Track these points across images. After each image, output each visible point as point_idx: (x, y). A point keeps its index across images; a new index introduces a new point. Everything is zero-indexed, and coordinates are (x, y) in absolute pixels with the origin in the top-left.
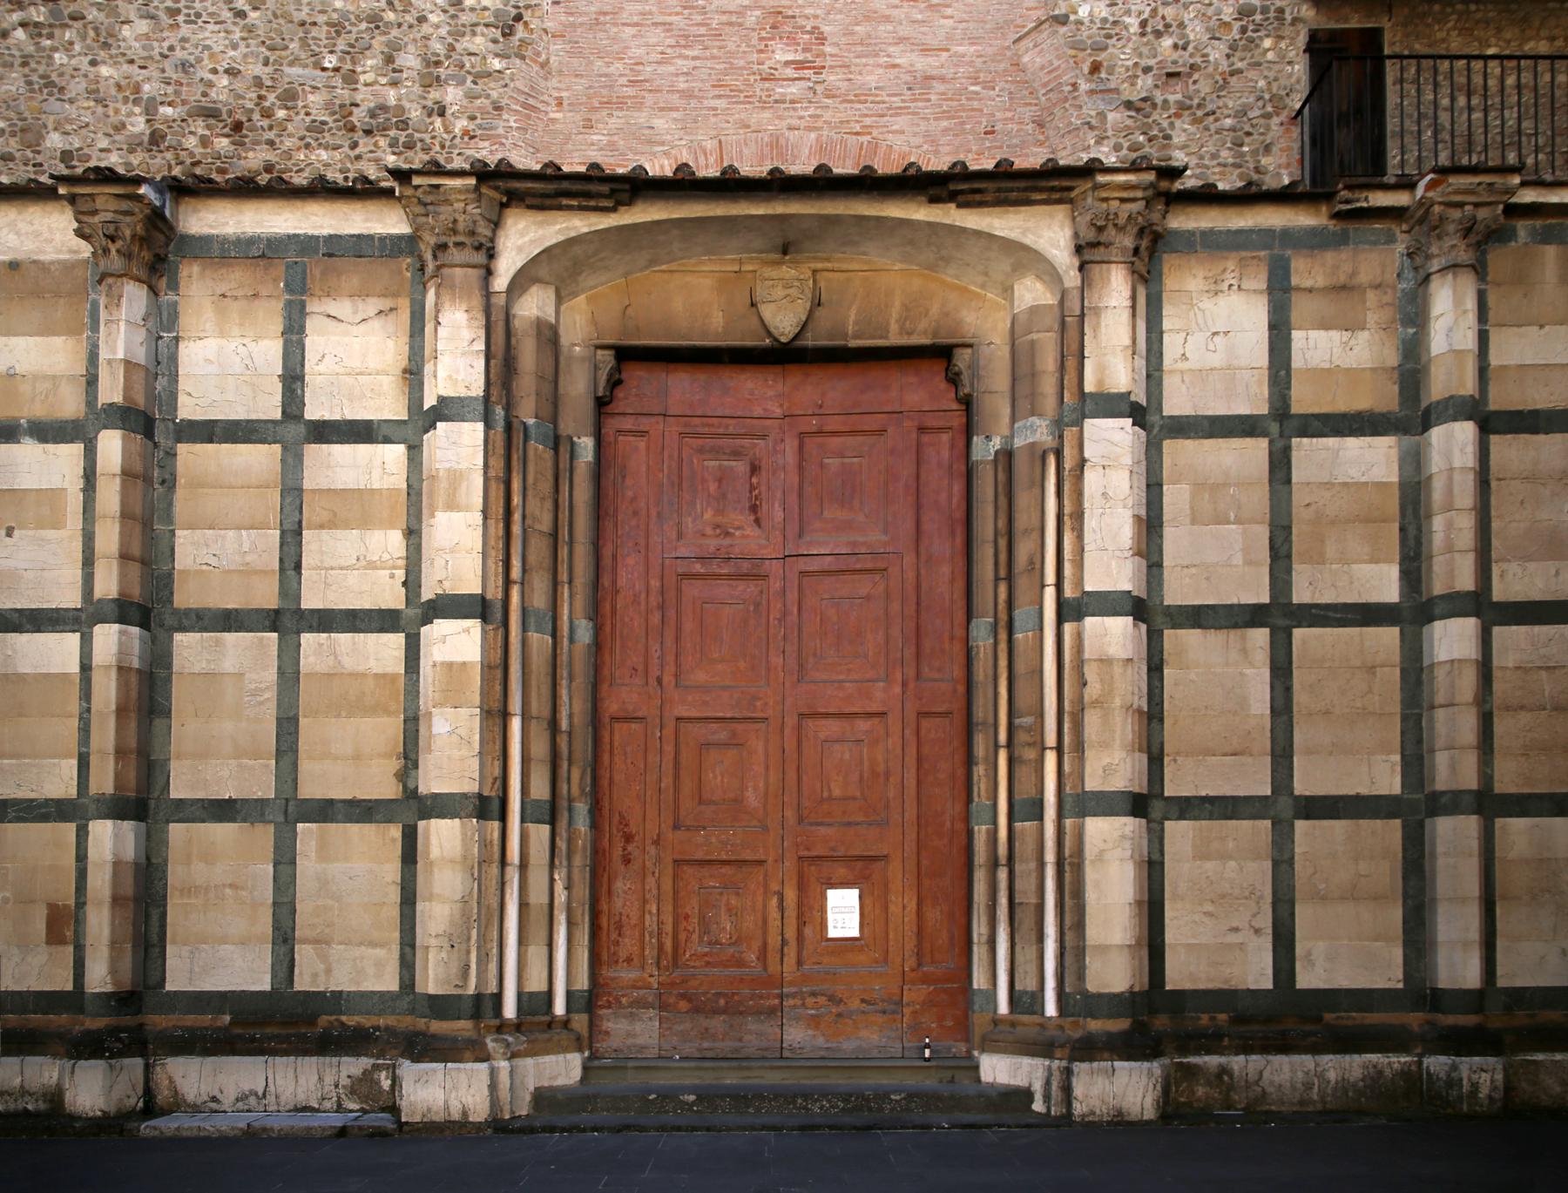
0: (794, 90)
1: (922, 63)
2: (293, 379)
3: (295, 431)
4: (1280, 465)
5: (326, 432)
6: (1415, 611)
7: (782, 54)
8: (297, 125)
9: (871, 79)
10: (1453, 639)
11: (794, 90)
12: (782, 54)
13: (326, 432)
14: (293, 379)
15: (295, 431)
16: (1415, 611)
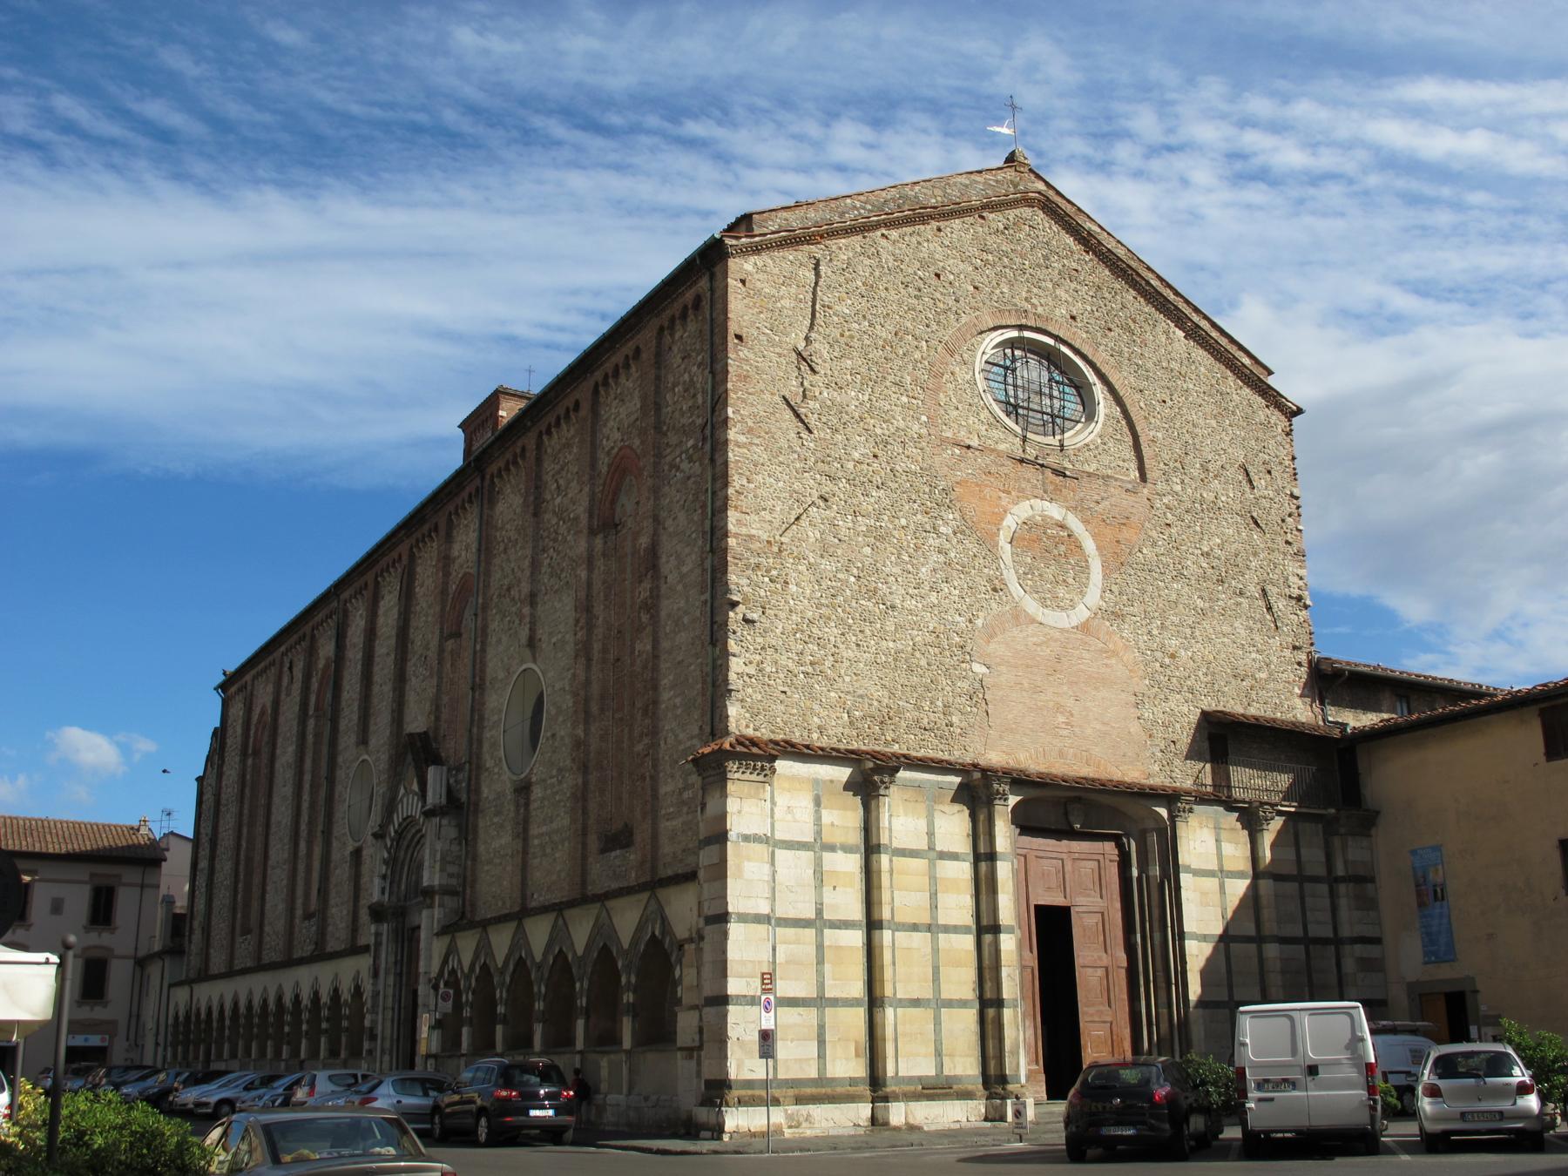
0: (1065, 733)
1: (1104, 728)
2: (931, 834)
3: (933, 855)
4: (1222, 887)
5: (943, 856)
6: (1259, 939)
7: (1061, 719)
8: (903, 724)
9: (1089, 731)
10: (1272, 950)
11: (1065, 733)
12: (1061, 719)
13: (943, 856)
14: (931, 834)
15: (933, 855)
16: (1259, 939)
